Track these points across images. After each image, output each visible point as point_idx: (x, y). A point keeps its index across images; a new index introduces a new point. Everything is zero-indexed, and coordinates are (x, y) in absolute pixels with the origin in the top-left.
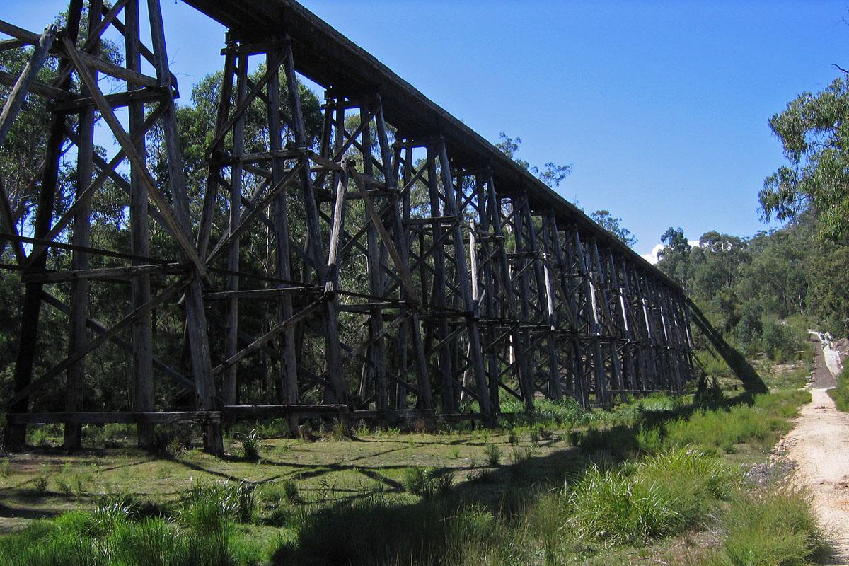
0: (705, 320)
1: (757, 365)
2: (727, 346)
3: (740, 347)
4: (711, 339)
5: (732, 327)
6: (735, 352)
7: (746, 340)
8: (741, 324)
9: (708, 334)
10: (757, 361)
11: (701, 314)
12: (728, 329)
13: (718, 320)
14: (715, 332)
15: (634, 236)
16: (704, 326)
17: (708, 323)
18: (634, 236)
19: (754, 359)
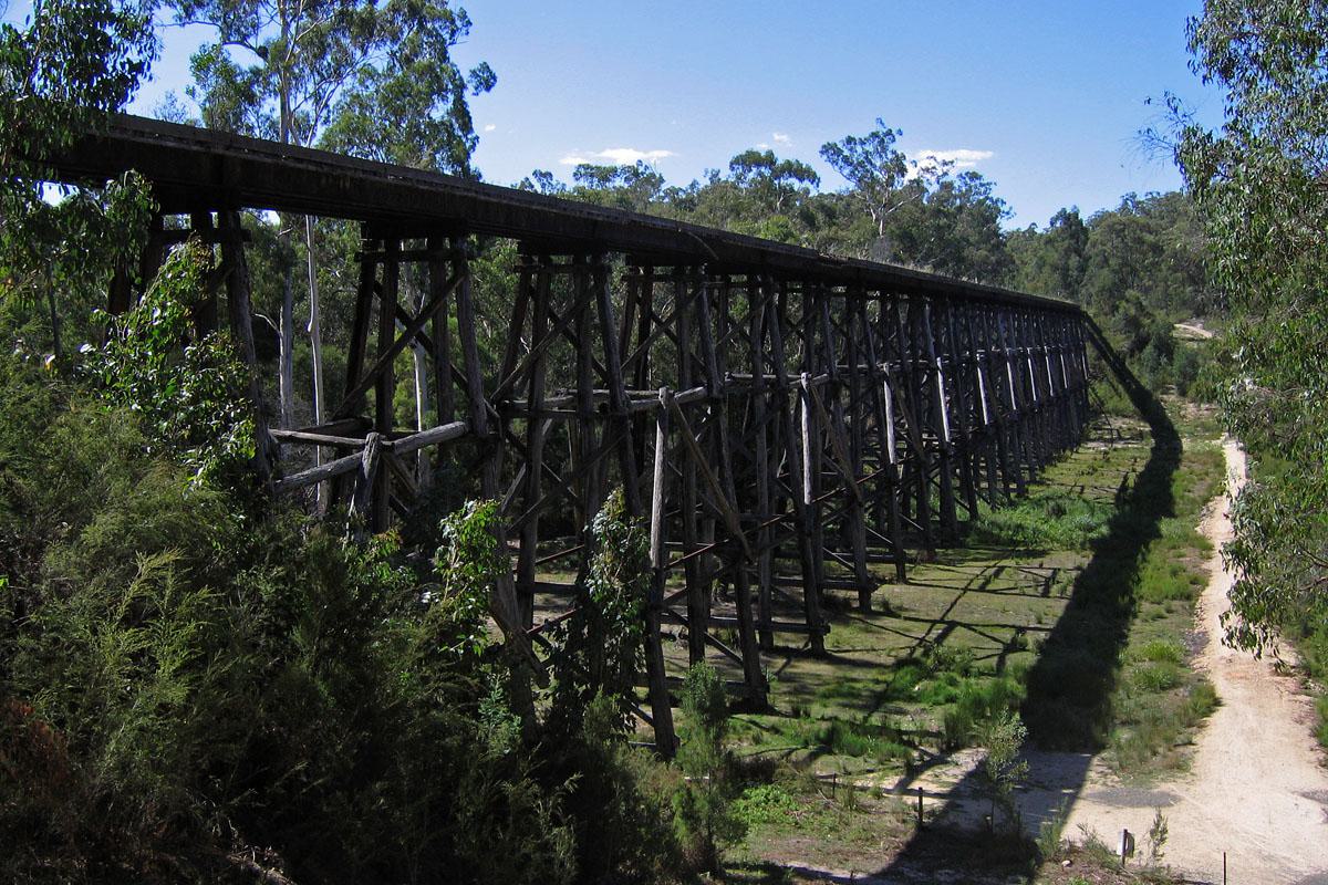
0: (1104, 340)
1: (1165, 402)
2: (1130, 375)
3: (1146, 381)
4: (1113, 366)
5: (1137, 352)
6: (1140, 388)
7: (1153, 370)
8: (1149, 349)
9: (1107, 360)
10: (1165, 396)
11: (1099, 332)
12: (1132, 353)
13: (1120, 342)
14: (1117, 357)
15: (1011, 208)
16: (1104, 349)
17: (1108, 345)
18: (1011, 208)
19: (1162, 394)
